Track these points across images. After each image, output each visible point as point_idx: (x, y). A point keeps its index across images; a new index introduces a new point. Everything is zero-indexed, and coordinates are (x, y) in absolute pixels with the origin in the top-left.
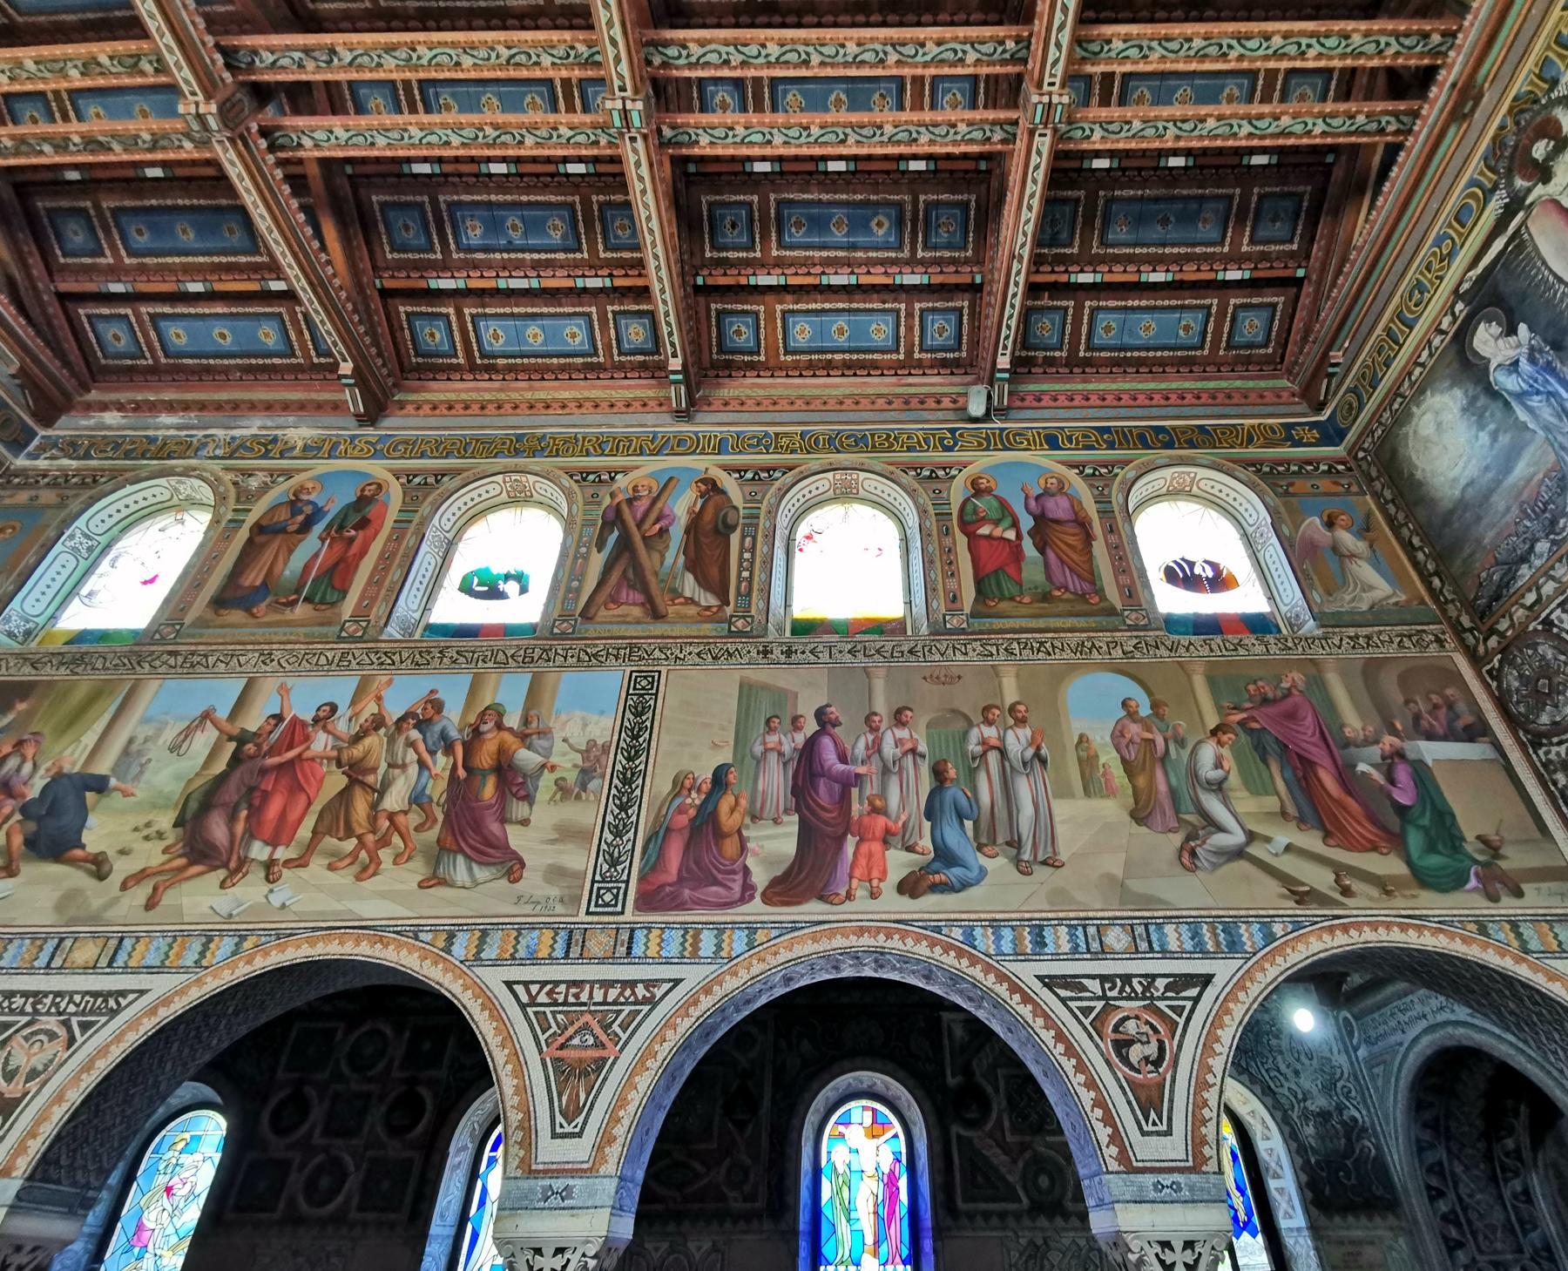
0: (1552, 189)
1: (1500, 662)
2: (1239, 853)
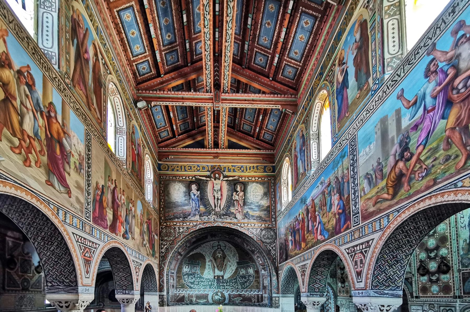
0: (214, 181)
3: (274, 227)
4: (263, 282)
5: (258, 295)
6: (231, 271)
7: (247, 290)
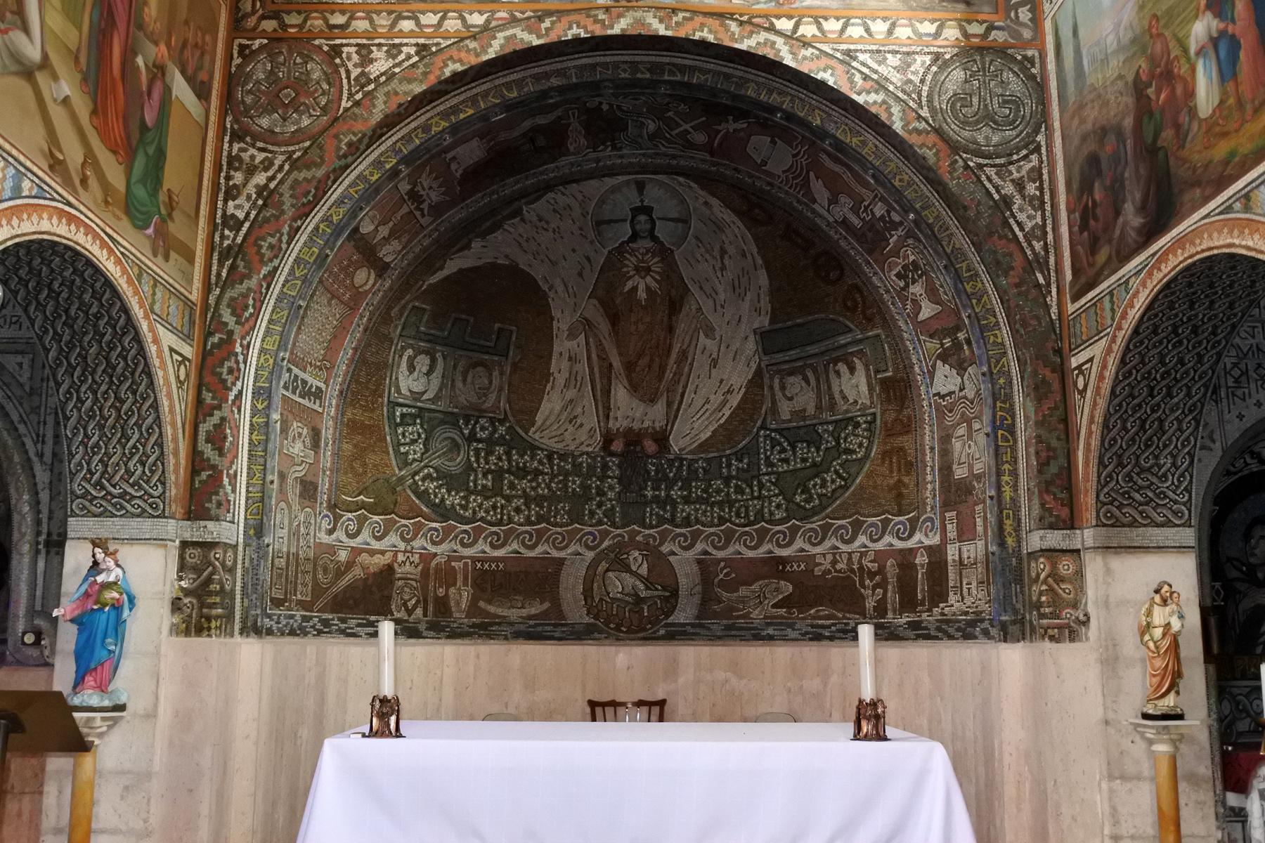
1: (262, 47)
2: (27, 73)
3: (1027, 44)
4: (946, 453)
5: (912, 552)
6: (716, 399)
7: (826, 528)
